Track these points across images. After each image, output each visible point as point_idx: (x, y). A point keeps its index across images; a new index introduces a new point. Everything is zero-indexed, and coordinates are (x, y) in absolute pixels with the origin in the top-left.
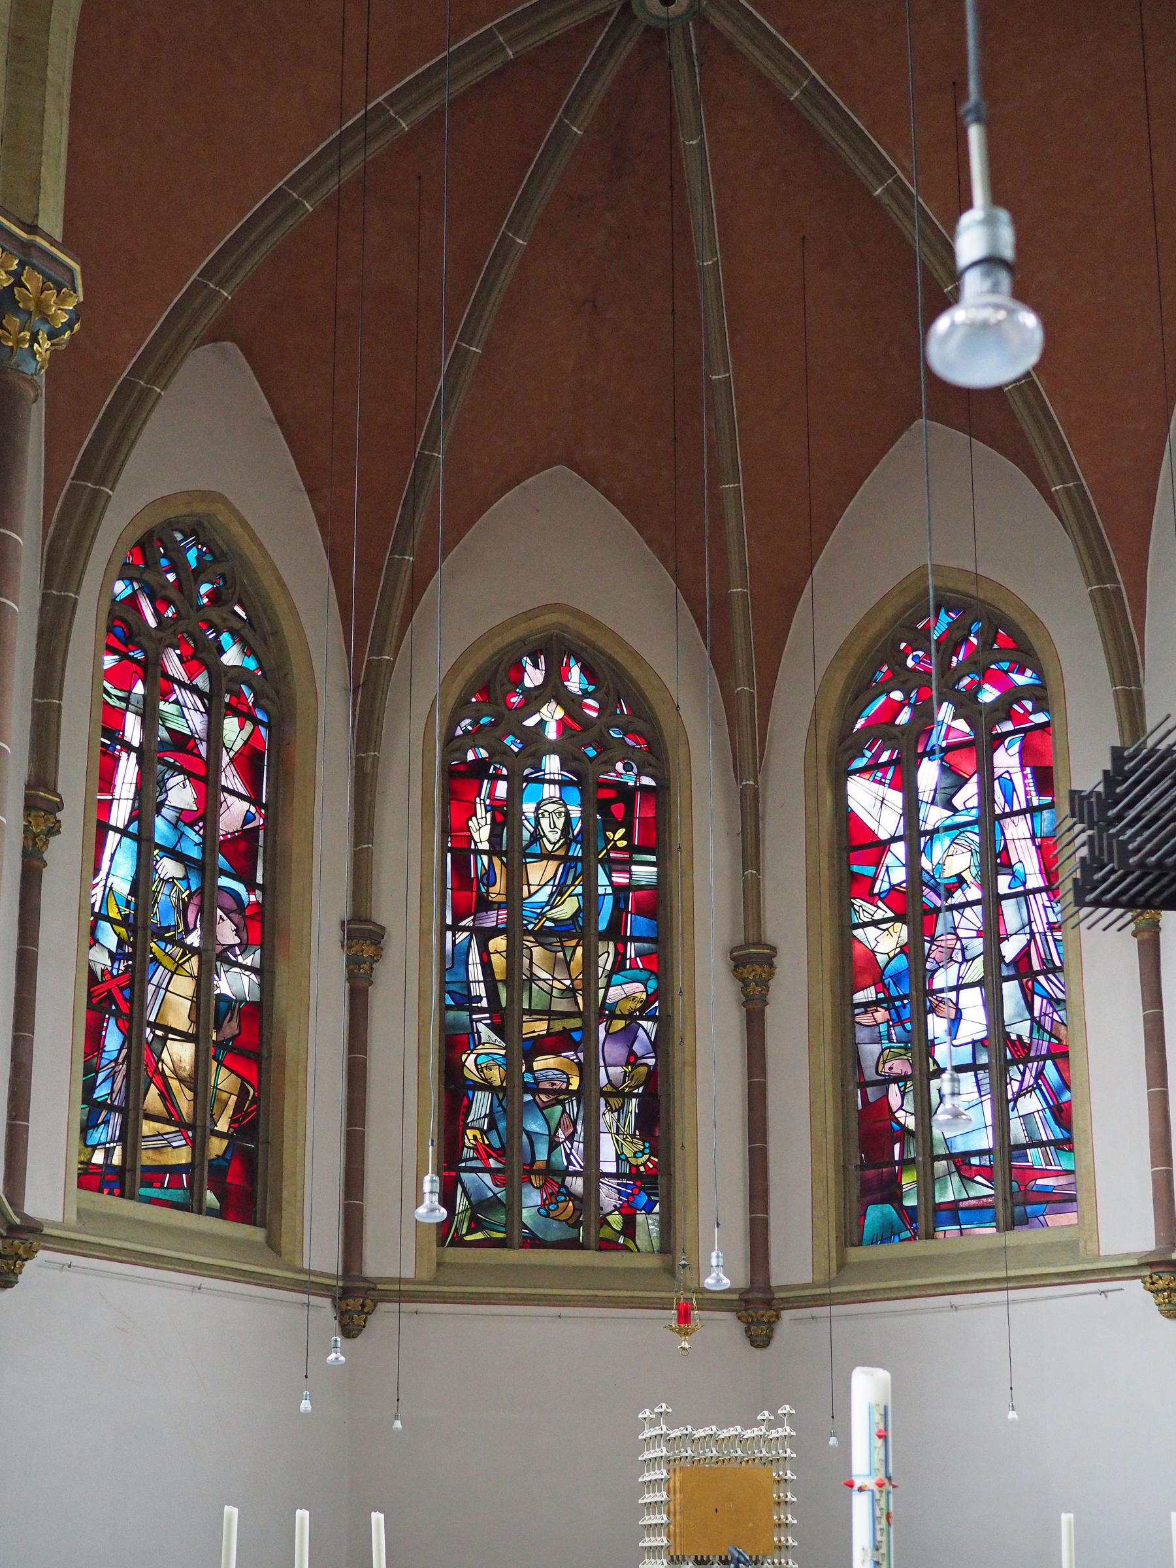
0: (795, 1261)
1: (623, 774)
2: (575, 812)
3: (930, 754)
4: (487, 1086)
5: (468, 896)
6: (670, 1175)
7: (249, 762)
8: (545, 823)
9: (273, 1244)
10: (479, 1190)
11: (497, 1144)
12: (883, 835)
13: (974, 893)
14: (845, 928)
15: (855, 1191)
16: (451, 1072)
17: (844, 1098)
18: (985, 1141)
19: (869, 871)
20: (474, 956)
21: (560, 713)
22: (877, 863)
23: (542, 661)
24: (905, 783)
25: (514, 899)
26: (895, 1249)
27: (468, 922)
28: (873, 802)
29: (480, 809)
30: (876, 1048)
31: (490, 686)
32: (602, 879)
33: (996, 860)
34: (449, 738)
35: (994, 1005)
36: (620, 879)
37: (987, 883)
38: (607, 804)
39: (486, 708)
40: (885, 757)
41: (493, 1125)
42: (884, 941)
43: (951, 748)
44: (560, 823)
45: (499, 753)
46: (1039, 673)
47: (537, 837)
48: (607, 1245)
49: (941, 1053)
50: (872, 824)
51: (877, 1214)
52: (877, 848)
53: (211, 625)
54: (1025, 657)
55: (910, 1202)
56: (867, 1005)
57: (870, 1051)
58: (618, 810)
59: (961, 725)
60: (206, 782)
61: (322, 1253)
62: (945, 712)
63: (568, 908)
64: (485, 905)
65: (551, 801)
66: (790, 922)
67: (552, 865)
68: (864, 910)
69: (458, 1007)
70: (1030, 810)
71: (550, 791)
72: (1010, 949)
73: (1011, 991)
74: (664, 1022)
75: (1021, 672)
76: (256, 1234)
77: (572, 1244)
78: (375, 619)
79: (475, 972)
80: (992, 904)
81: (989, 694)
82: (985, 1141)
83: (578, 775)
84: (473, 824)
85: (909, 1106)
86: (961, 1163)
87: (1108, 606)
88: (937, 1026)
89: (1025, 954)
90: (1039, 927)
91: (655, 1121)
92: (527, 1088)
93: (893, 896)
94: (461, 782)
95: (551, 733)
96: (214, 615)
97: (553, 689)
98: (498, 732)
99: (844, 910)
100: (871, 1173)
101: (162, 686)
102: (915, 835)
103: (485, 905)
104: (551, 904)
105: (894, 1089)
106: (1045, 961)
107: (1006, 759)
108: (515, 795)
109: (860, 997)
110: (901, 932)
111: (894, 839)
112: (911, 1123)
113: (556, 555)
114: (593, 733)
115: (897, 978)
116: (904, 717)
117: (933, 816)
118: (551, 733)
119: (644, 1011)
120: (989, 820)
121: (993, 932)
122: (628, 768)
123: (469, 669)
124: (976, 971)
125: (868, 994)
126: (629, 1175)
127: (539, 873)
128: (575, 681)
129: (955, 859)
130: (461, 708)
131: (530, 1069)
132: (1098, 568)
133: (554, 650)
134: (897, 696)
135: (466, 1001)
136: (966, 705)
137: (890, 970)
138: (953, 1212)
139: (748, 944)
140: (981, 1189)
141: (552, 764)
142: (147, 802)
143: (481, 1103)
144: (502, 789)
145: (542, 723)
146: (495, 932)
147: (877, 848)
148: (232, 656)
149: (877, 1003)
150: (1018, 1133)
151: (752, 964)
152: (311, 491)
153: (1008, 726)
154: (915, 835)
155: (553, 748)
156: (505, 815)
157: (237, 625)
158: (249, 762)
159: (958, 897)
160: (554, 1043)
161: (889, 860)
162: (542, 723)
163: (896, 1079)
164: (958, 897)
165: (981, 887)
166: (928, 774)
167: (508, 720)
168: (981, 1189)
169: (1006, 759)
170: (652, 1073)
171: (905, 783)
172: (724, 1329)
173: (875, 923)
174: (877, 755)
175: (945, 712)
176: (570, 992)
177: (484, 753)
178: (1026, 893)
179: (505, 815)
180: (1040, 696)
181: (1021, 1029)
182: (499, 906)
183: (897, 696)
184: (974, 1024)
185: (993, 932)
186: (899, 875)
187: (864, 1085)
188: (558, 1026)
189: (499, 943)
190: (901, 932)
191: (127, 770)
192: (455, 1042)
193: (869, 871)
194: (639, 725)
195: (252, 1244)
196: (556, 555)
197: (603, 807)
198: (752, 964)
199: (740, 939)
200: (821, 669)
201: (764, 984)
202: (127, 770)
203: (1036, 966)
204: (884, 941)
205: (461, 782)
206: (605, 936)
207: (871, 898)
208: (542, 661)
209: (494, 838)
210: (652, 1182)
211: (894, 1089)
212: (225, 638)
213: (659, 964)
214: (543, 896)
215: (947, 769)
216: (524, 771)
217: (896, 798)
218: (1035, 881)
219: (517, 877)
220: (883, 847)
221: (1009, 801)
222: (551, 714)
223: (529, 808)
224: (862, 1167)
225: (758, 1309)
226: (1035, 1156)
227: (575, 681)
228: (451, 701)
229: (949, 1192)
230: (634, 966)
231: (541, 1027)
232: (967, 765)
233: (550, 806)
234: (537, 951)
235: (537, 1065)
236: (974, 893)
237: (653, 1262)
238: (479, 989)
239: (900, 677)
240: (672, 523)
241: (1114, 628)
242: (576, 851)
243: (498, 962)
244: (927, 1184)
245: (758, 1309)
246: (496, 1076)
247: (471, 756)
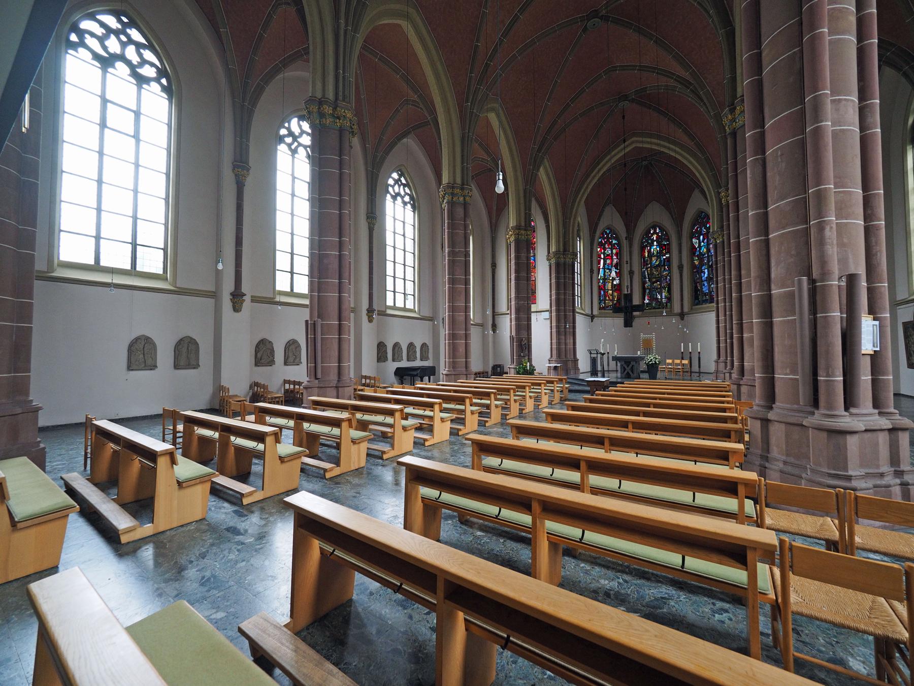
0: (686, 310)
5: (645, 263)
7: (617, 254)
14: (693, 260)
24: (699, 239)
25: (651, 263)
33: (709, 250)
60: (612, 260)
83: (659, 245)
91: (669, 291)
97: (655, 232)
101: (605, 249)
102: (700, 247)
113: (655, 213)
127: (654, 259)
130: (643, 238)
133: (654, 228)
142: (604, 264)
148: (614, 242)
151: (681, 267)
154: (700, 247)
156: (649, 252)
158: (617, 254)
172: (678, 318)
179: (649, 252)
191: (602, 261)
196: (655, 213)
198: (681, 267)
202: (602, 261)
204: (696, 263)
205: (643, 249)
210: (669, 299)
216: (652, 245)
219: (651, 260)
222: (655, 237)
225: (682, 315)
233: (655, 248)
240: (667, 206)
245: (682, 315)
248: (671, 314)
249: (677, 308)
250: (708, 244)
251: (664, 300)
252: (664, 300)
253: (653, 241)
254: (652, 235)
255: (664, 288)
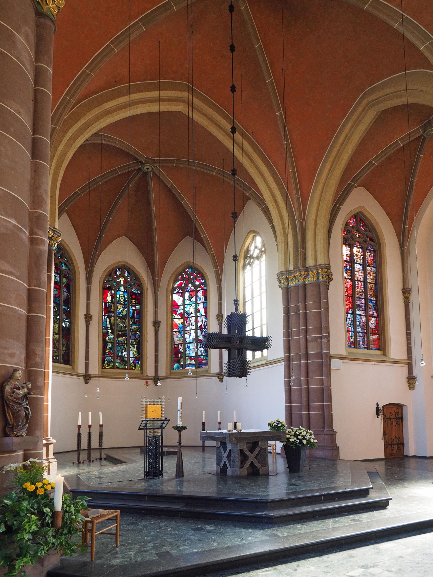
0: (162, 372)
1: (134, 290)
2: (126, 296)
3: (187, 292)
4: (110, 342)
6: (142, 358)
8: (121, 298)
9: (73, 368)
10: (109, 360)
11: (112, 352)
12: (179, 304)
13: (193, 315)
15: (173, 361)
16: (104, 340)
17: (172, 346)
18: (194, 354)
19: (177, 310)
20: (108, 320)
21: (123, 279)
22: (178, 309)
23: (120, 270)
25: (115, 311)
26: (179, 371)
27: (107, 315)
28: (178, 299)
29: (109, 295)
30: (177, 339)
31: (111, 274)
32: (131, 308)
34: (104, 283)
35: (196, 333)
36: (134, 308)
37: (196, 313)
38: (132, 295)
39: (110, 278)
40: (180, 291)
41: (111, 349)
42: (179, 321)
43: (191, 291)
44: (123, 298)
45: (112, 285)
46: (205, 281)
47: (119, 300)
48: (131, 369)
49: (188, 340)
50: (177, 302)
51: (176, 365)
52: (178, 307)
53: (60, 262)
54: (203, 277)
55: (182, 363)
56: (175, 332)
57: (176, 339)
58: (134, 296)
59: (193, 288)
61: (81, 370)
62: (190, 285)
63: (124, 313)
64: (110, 312)
65: (122, 294)
66: (162, 317)
67: (122, 306)
68: (175, 316)
69: (105, 329)
70: (203, 303)
71: (121, 293)
72: (199, 325)
73: (199, 331)
74: (141, 333)
75: (203, 280)
76: (70, 367)
77: (125, 369)
78: (90, 263)
79: (108, 323)
80: (196, 317)
81: (197, 283)
82: (194, 354)
84: (108, 298)
85: (182, 348)
86: (190, 358)
87: (217, 273)
88: (187, 336)
89: (201, 325)
90: (204, 321)
92: (117, 343)
93: (181, 315)
94: (105, 290)
95: (122, 283)
96: (61, 260)
97: (122, 275)
98: (113, 282)
99: (172, 316)
100: (175, 359)
102: (184, 305)
103: (110, 312)
104: (122, 312)
105: (180, 345)
106: (205, 327)
107: (200, 294)
108: (115, 293)
109: (174, 330)
110: (182, 320)
111: (181, 305)
112: (182, 351)
114: (129, 283)
115: (181, 328)
116: (183, 285)
117: (187, 302)
118: (122, 283)
119: (138, 330)
120: (196, 303)
121: (196, 322)
122: (135, 289)
123: (107, 271)
124: (193, 328)
125: (176, 330)
126: (135, 357)
127: (119, 307)
128: (126, 274)
129: (190, 309)
131: (118, 340)
132: (216, 267)
134: (182, 282)
135: (106, 328)
136: (193, 285)
137: (180, 326)
138: (189, 365)
139: (156, 321)
140: (193, 362)
141: (122, 288)
143: (109, 345)
144: (113, 292)
145: (120, 281)
146: (112, 316)
147: (178, 307)
149: (177, 331)
150: (199, 353)
151: (156, 324)
152: (79, 239)
153: (200, 289)
154: (184, 305)
155: (122, 285)
156: (113, 296)
157: (65, 262)
159: (191, 316)
160: (122, 336)
161: (180, 308)
162: (120, 281)
163: (180, 344)
164: (191, 316)
165: (195, 314)
166: (187, 295)
167: (114, 280)
168: (193, 362)
169: (200, 294)
170: (139, 341)
171: (183, 295)
173: (177, 319)
174: (178, 291)
175: (190, 285)
176: (125, 327)
177: (110, 285)
178: (202, 316)
180: (205, 284)
181: (201, 338)
182: (112, 312)
183: (182, 282)
184: (192, 337)
185: (196, 322)
186: (182, 311)
187: (175, 344)
188: (123, 333)
189: (112, 318)
190: (182, 320)
192: (105, 335)
193: (177, 310)
194: (137, 282)
195: (69, 369)
197: (131, 296)
199: (155, 320)
200: (170, 275)
201: (158, 327)
203: (203, 328)
206: (131, 318)
207: (177, 314)
208: (120, 270)
209: (112, 300)
211: (180, 345)
212: (63, 265)
213: (141, 323)
214: (120, 311)
215: (190, 295)
217: (181, 298)
218: (204, 314)
219: (116, 307)
220: (179, 306)
221: (200, 301)
222: (122, 280)
223: (118, 295)
224: (174, 357)
226: (202, 357)
227: (126, 274)
228: (104, 277)
229: (188, 362)
230: (136, 323)
231: (120, 333)
232: (192, 293)
234: (119, 320)
235: (119, 339)
236: (193, 315)
237: (139, 372)
238: (109, 326)
239: (182, 279)
241: (217, 276)
242: (126, 303)
243: (112, 321)
244: (185, 361)
246: (112, 340)
247: (107, 286)
248: (142, 376)
249: (150, 371)
250: (196, 303)
251: (131, 361)
252: (131, 361)
253: (119, 284)
254: (118, 277)
255: (133, 344)
